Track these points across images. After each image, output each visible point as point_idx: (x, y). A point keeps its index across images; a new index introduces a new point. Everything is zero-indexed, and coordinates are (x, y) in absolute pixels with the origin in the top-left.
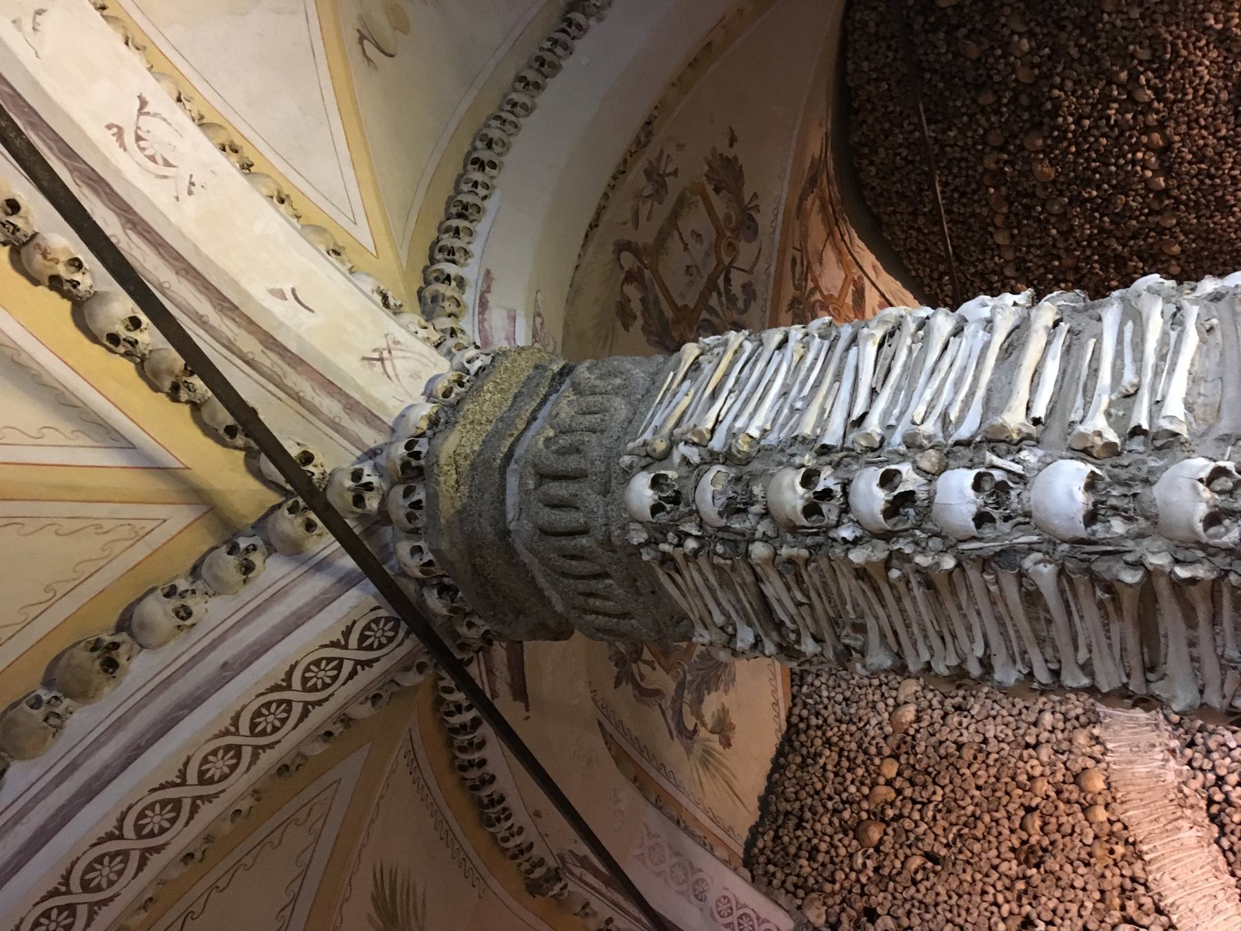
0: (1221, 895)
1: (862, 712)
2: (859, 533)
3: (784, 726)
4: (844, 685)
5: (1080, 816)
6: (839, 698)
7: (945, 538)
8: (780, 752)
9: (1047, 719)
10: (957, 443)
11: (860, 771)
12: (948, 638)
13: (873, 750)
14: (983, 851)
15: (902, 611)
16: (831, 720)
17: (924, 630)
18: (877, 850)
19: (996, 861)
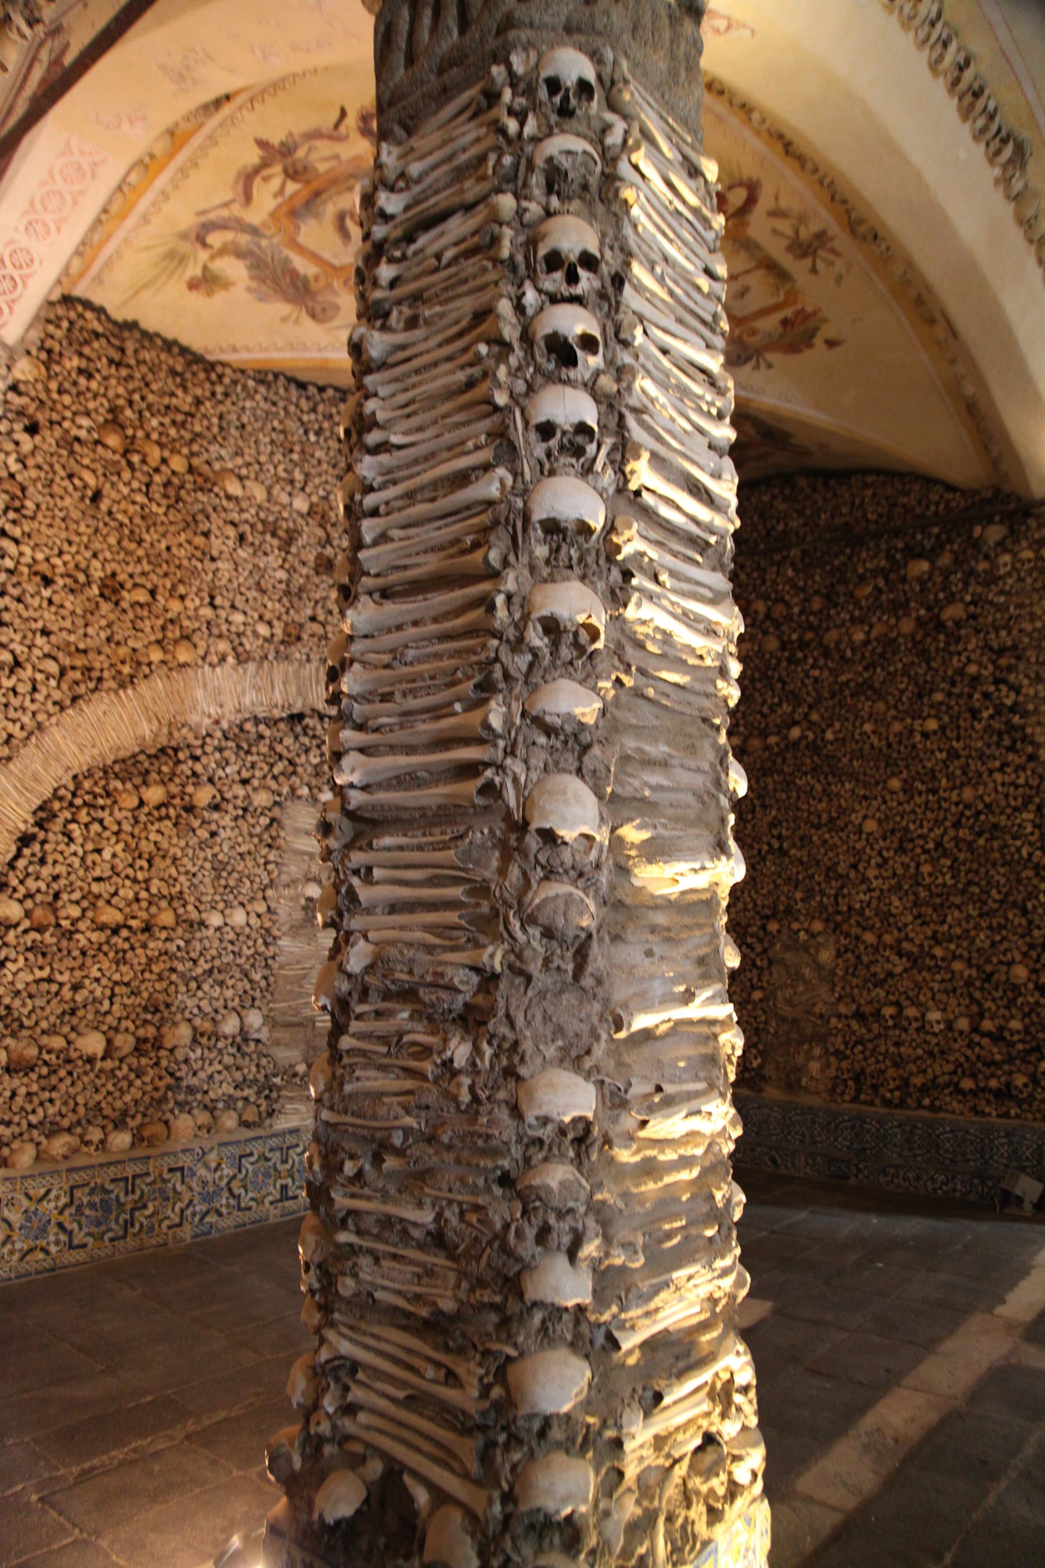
0: (96, 751)
1: (232, 441)
2: (530, 311)
3: (210, 358)
4: (258, 425)
5: (153, 638)
6: (245, 419)
7: (527, 395)
8: (184, 351)
9: (238, 618)
10: (621, 417)
11: (173, 432)
12: (407, 410)
13: (195, 448)
14: (110, 547)
15: (435, 364)
16: (221, 408)
17: (414, 386)
18: (97, 442)
19: (101, 557)
